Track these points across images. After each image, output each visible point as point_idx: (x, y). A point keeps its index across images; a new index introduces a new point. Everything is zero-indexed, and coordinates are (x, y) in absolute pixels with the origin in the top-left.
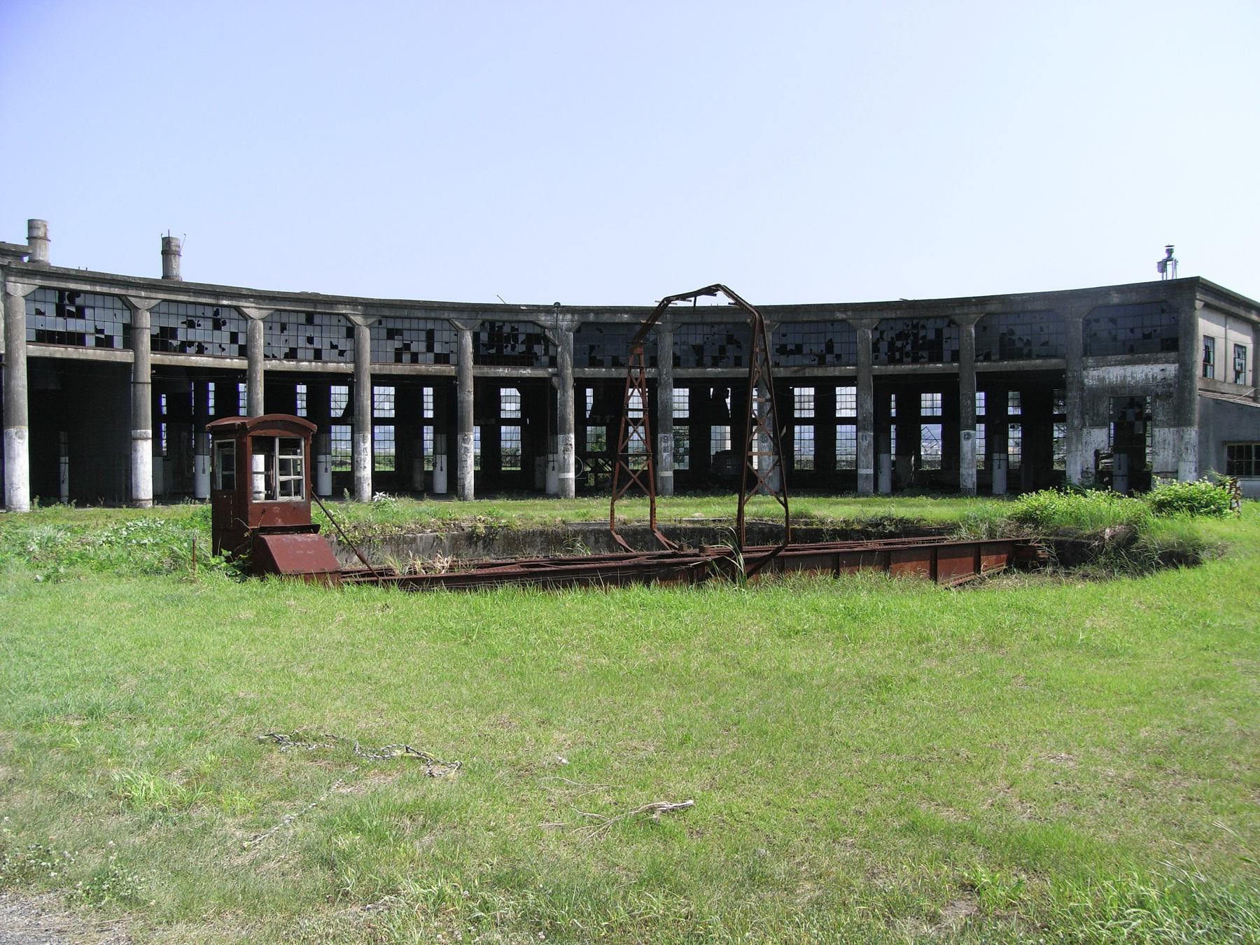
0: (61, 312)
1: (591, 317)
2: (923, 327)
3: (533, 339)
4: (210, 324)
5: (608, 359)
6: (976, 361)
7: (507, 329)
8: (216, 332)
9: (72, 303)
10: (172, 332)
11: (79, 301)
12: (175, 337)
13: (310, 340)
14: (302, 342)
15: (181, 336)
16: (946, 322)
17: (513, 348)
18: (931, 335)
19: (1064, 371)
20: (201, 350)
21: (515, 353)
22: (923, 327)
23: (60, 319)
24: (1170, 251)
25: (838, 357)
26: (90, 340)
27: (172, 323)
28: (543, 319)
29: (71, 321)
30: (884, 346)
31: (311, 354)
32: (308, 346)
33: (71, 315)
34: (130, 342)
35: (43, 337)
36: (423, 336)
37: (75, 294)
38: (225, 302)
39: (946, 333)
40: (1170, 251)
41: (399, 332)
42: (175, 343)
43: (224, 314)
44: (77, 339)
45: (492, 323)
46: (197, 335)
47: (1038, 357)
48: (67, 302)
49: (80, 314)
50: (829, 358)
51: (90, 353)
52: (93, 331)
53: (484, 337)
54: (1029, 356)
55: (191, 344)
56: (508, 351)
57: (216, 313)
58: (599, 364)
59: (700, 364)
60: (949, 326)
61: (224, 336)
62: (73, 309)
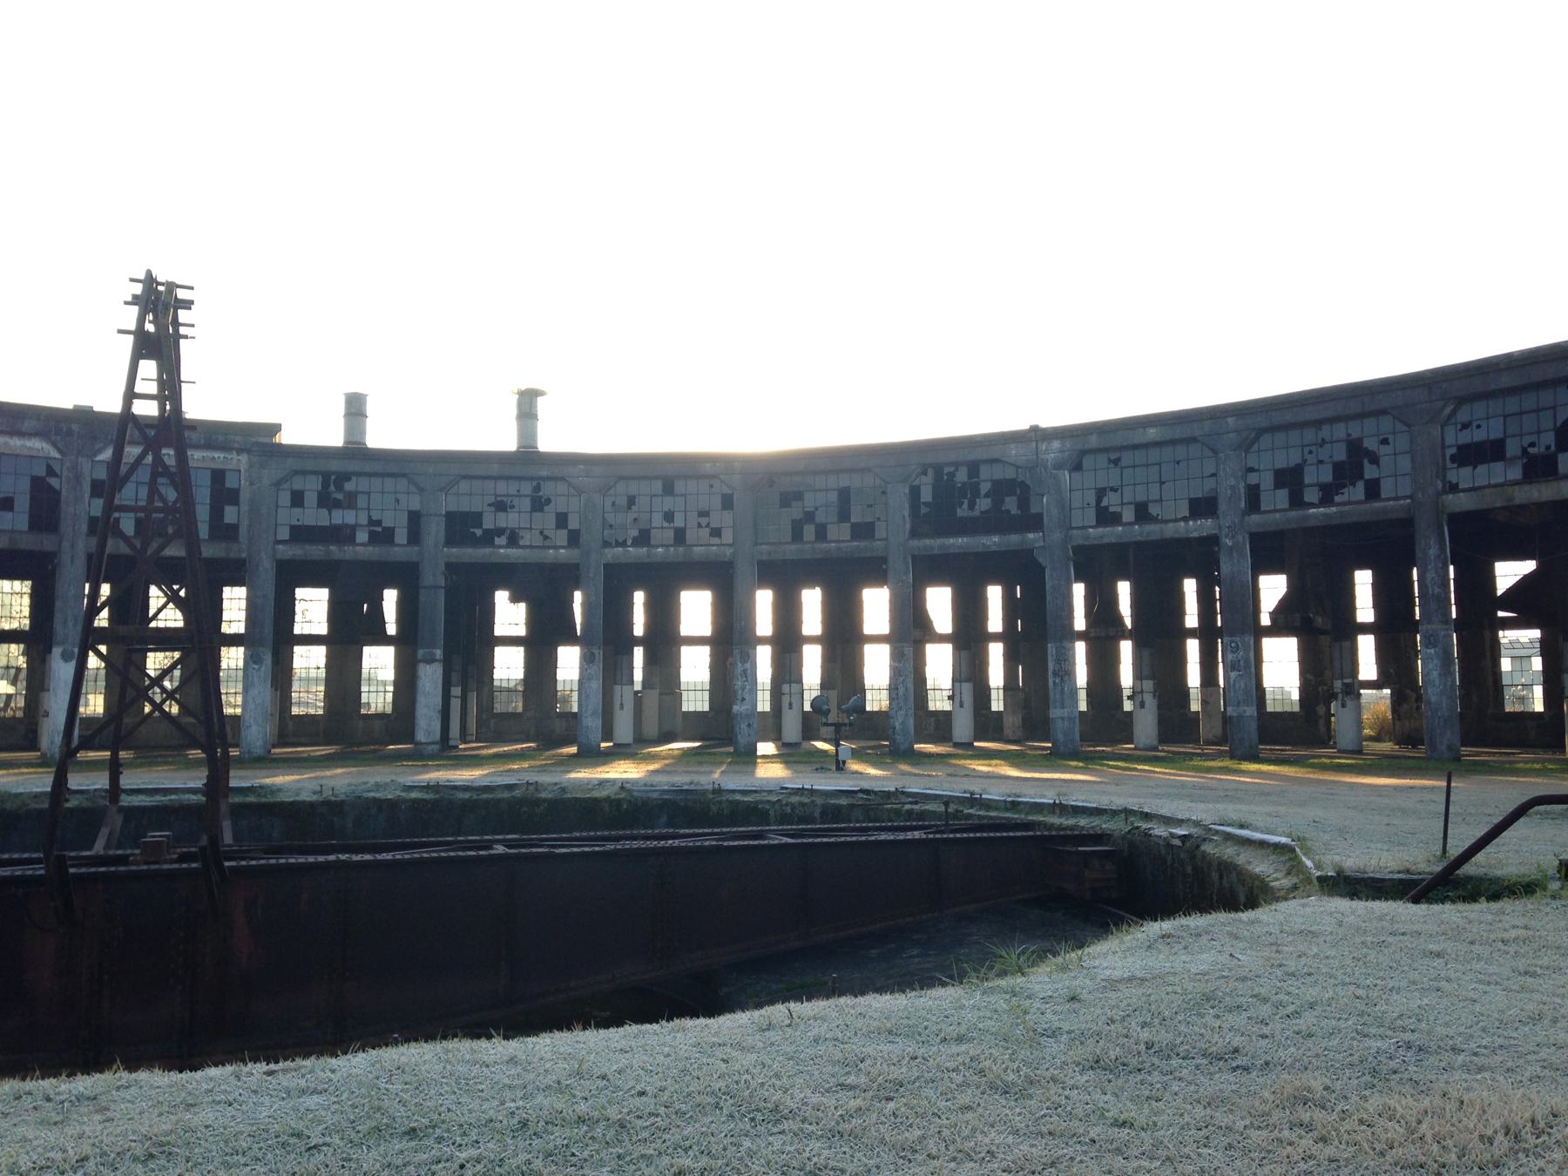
0: (325, 501)
1: (1094, 441)
3: (1001, 489)
4: (526, 504)
5: (1128, 515)
7: (962, 476)
8: (538, 514)
9: (339, 488)
10: (477, 518)
11: (349, 486)
12: (480, 526)
13: (669, 517)
14: (657, 520)
15: (488, 523)
17: (972, 506)
20: (513, 540)
21: (976, 513)
23: (325, 512)
26: (362, 536)
27: (476, 505)
28: (1013, 451)
31: (669, 535)
32: (666, 524)
33: (337, 505)
34: (415, 536)
35: (300, 534)
36: (833, 497)
37: (347, 477)
41: (798, 496)
42: (479, 532)
43: (547, 490)
45: (938, 469)
48: (332, 488)
49: (350, 502)
52: (366, 522)
53: (926, 495)
55: (500, 532)
56: (962, 512)
57: (537, 488)
58: (1115, 519)
61: (547, 519)
62: (340, 496)
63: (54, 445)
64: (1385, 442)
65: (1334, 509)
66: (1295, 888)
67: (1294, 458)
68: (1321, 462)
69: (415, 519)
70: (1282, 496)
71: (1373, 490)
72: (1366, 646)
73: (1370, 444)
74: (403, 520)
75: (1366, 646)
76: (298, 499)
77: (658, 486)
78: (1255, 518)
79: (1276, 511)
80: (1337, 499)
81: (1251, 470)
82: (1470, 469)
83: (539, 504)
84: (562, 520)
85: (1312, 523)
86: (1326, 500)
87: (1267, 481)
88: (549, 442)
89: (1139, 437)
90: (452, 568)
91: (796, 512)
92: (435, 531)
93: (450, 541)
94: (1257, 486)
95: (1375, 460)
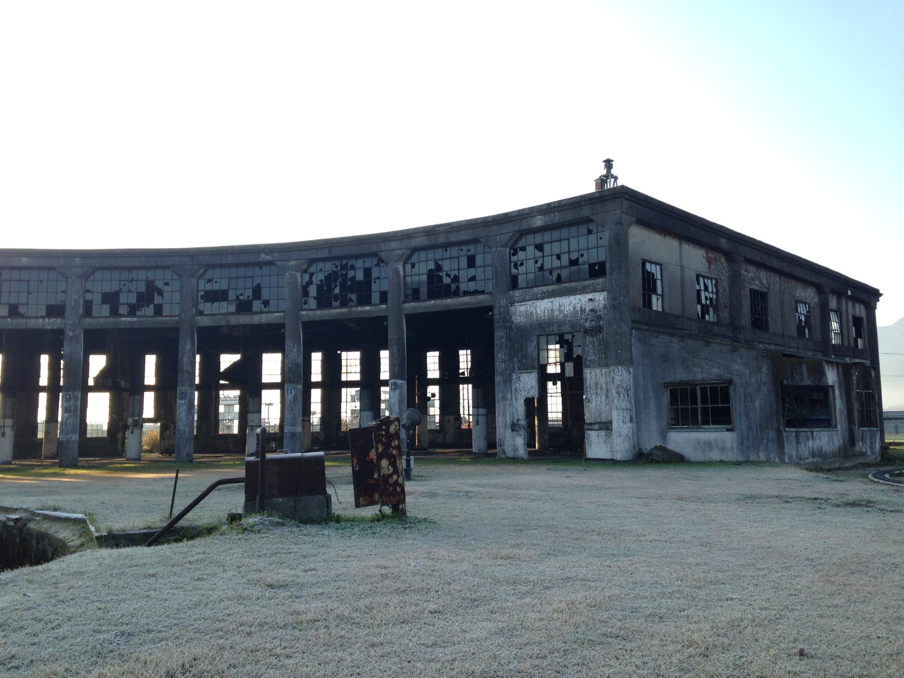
2: (353, 267)
6: (405, 302)
16: (375, 261)
18: (360, 276)
19: (491, 308)
22: (353, 267)
24: (609, 164)
25: (266, 303)
30: (313, 290)
39: (375, 273)
40: (609, 164)
47: (466, 293)
50: (257, 305)
54: (457, 293)
60: (378, 265)
64: (167, 284)
65: (136, 319)
66: (82, 545)
67: (115, 287)
68: (130, 291)
70: (106, 309)
71: (158, 310)
72: (149, 399)
73: (159, 284)
75: (149, 399)
78: (88, 320)
79: (101, 317)
80: (138, 313)
81: (88, 291)
82: (210, 304)
85: (123, 326)
86: (132, 313)
87: (97, 299)
89: (15, 262)
94: (91, 302)
95: (161, 293)
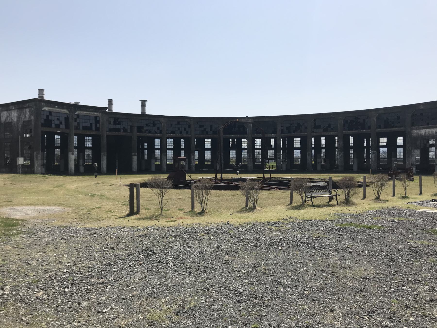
0: (115, 123)
4: (152, 125)
10: (142, 127)
11: (119, 120)
13: (179, 129)
18: (362, 121)
20: (150, 132)
26: (122, 130)
29: (117, 126)
31: (179, 132)
34: (131, 131)
35: (110, 130)
37: (118, 119)
38: (156, 119)
41: (203, 126)
44: (118, 130)
46: (149, 128)
47: (396, 127)
49: (119, 124)
51: (122, 133)
54: (393, 127)
59: (289, 132)
63: (69, 111)
69: (131, 127)
74: (129, 127)
76: (110, 124)
77: (176, 123)
78: (283, 134)
83: (154, 125)
84: (158, 128)
88: (149, 112)
90: (139, 137)
91: (202, 129)
92: (135, 130)
93: (138, 132)
